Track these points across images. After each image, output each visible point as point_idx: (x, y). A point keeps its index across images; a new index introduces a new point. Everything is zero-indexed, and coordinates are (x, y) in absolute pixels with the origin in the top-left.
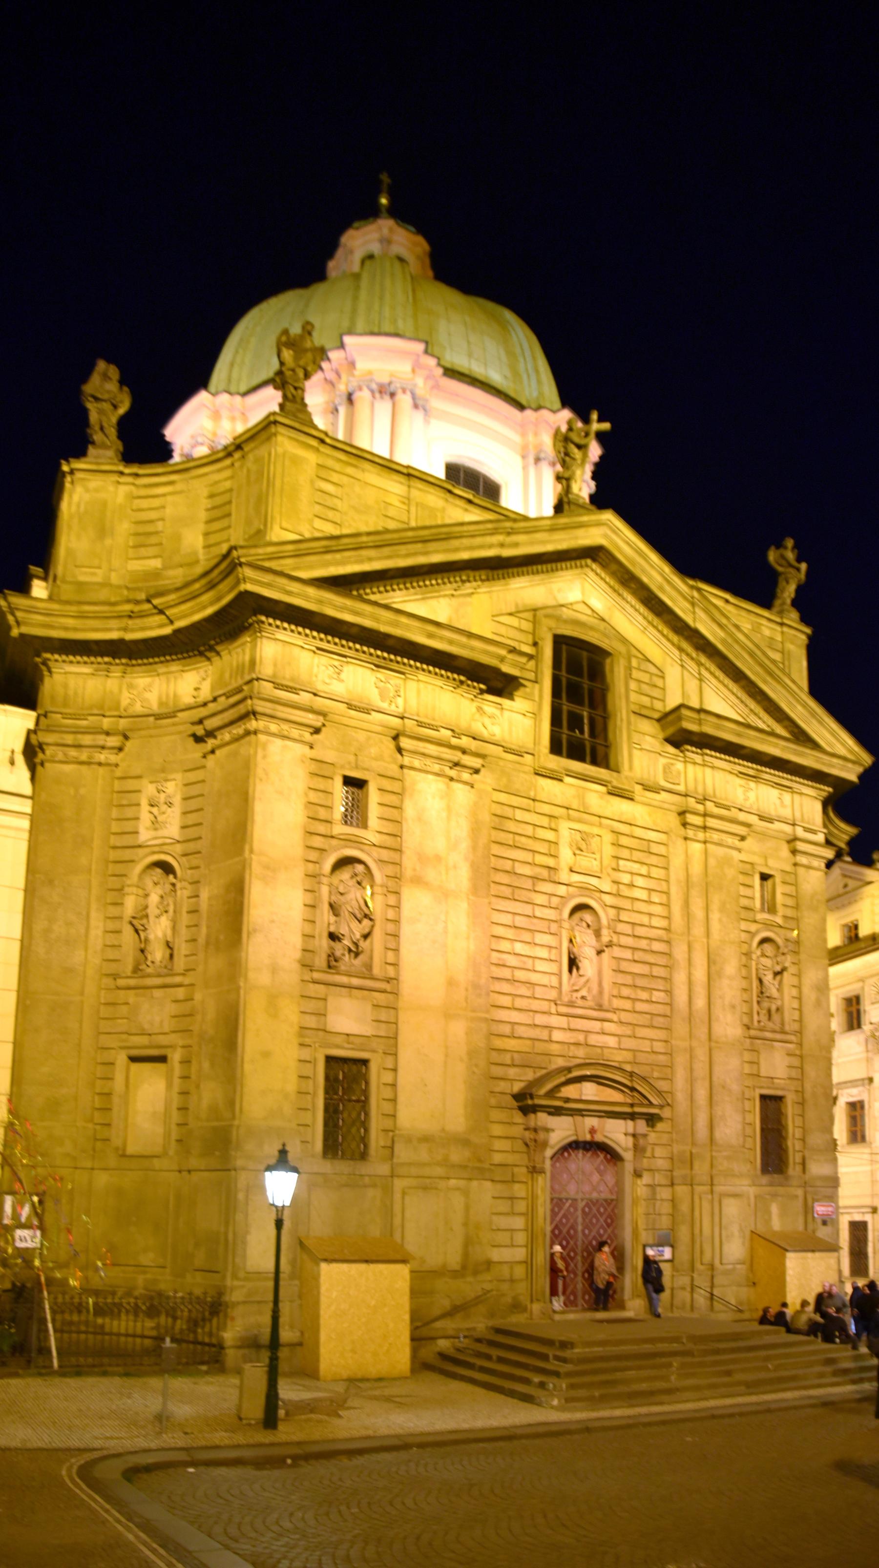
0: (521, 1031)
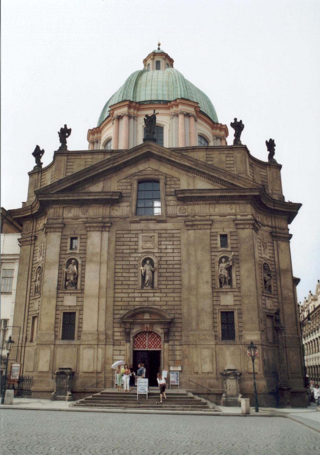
0: (124, 299)
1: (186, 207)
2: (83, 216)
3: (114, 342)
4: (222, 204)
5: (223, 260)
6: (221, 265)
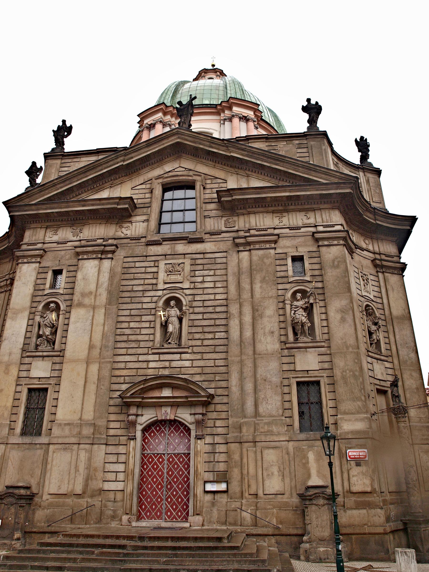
0: (130, 365)
1: (235, 218)
2: (75, 239)
3: (107, 439)
4: (294, 211)
5: (299, 295)
6: (295, 303)
